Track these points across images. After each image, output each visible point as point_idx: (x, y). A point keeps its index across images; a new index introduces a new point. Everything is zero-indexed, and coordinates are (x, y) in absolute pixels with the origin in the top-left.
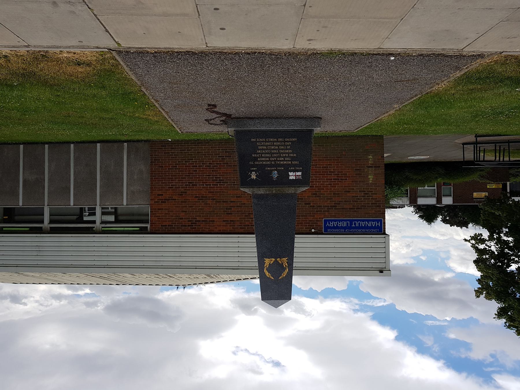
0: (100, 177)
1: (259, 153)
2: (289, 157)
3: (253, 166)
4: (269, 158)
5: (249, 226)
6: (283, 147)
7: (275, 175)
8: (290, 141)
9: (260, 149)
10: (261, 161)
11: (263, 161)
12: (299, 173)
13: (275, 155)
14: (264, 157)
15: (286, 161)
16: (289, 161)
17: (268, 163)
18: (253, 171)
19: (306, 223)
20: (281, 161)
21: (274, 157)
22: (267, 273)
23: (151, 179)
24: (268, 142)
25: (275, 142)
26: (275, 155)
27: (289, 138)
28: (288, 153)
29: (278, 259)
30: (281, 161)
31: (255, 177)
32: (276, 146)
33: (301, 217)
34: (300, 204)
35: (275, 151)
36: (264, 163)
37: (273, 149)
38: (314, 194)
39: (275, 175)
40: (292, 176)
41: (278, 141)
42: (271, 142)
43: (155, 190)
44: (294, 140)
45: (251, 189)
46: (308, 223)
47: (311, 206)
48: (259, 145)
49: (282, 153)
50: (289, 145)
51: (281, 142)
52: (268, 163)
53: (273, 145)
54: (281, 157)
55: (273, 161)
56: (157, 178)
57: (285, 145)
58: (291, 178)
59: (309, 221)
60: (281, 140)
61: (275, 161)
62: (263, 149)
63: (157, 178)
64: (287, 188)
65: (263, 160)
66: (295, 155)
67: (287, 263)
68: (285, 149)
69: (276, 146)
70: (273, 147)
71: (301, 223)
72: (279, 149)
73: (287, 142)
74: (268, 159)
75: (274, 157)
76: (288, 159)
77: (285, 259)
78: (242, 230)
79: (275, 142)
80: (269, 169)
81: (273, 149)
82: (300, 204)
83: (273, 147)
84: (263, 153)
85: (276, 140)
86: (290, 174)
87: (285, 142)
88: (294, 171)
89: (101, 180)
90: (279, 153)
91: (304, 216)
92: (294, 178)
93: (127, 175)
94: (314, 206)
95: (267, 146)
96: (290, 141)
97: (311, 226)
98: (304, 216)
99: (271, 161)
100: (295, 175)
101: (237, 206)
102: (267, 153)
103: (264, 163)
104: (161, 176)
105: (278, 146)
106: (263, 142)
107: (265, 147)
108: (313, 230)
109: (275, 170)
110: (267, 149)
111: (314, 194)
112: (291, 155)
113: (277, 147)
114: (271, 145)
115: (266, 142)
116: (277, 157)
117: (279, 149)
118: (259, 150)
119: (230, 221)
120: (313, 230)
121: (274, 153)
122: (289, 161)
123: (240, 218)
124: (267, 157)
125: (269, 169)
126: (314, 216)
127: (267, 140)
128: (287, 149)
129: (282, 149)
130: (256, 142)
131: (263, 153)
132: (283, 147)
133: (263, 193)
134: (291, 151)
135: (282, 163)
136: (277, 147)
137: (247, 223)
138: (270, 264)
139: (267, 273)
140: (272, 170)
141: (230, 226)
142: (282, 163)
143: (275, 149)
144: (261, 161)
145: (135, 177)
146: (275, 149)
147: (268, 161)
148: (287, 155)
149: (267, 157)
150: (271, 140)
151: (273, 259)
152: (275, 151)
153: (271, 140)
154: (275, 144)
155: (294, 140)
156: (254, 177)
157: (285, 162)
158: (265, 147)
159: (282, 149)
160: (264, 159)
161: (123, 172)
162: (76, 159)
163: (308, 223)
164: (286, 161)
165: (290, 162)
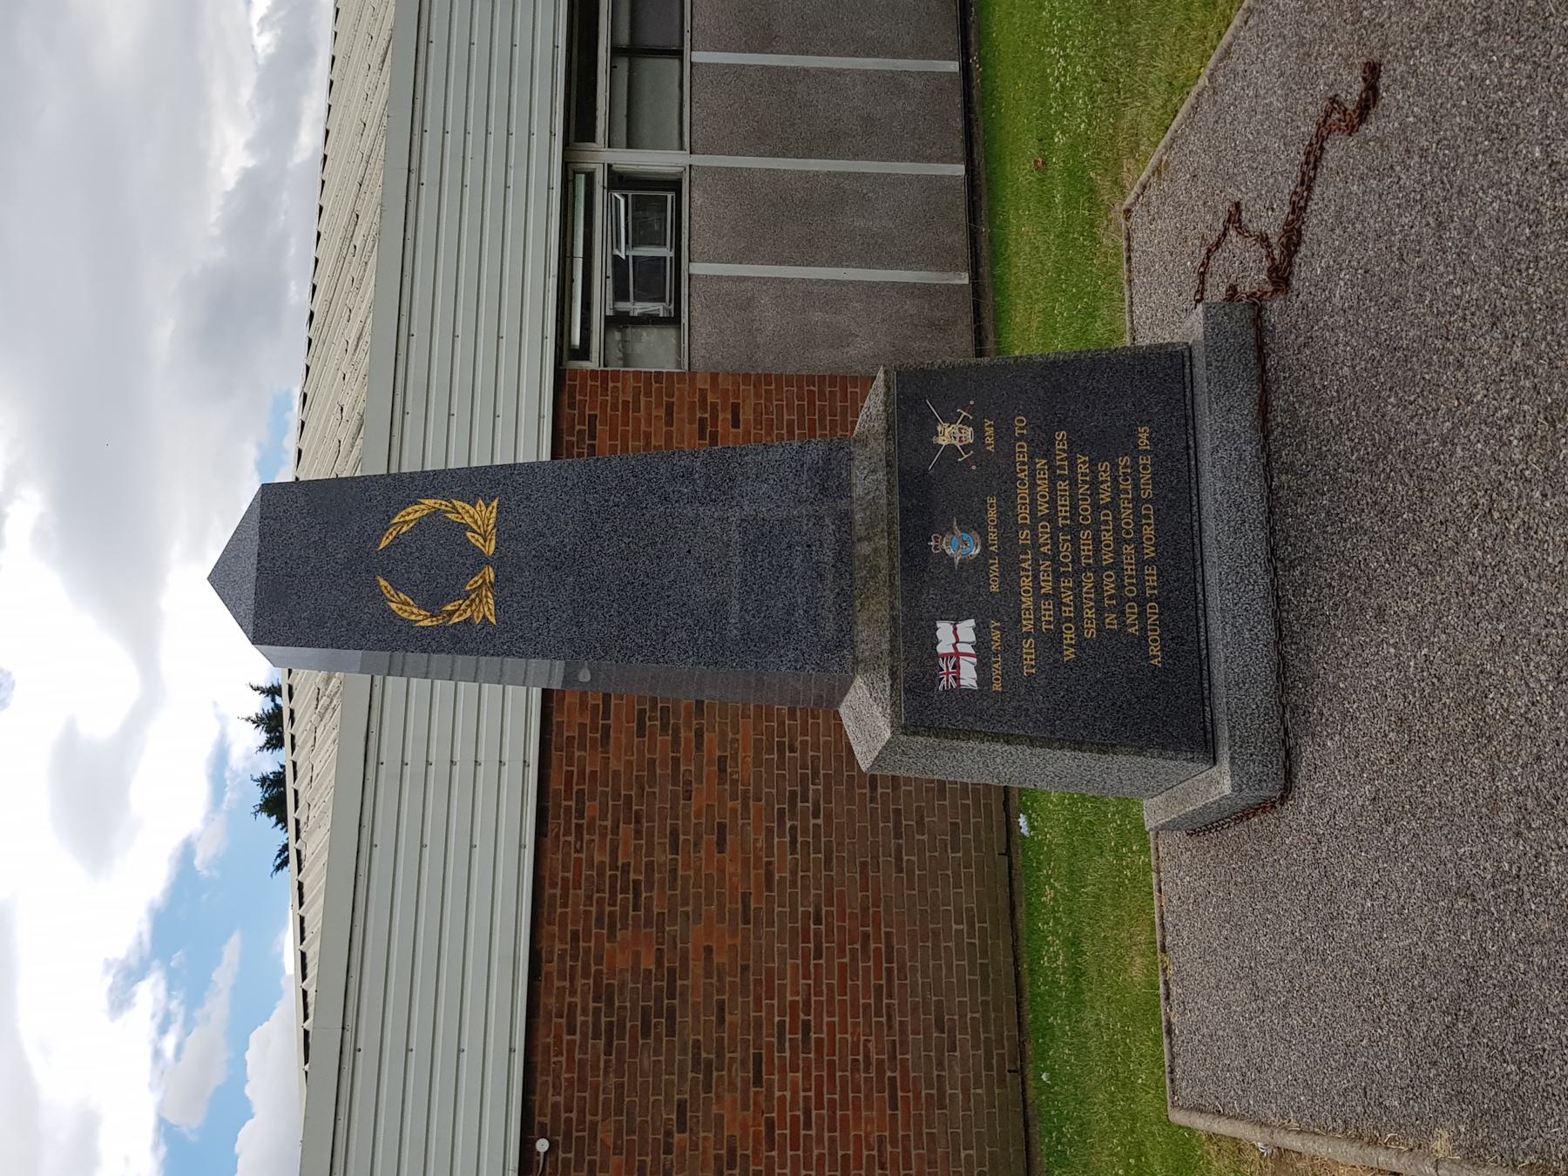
0: (817, 174)
1: (1073, 466)
2: (1059, 621)
3: (1004, 433)
4: (1052, 518)
5: (581, 815)
6: (1110, 589)
7: (960, 546)
8: (1143, 629)
9: (1094, 473)
10: (1032, 476)
11: (1033, 485)
12: (969, 676)
13: (1065, 548)
14: (1053, 489)
15: (1037, 609)
16: (1038, 620)
17: (1024, 513)
18: (979, 433)
19: (582, 1112)
20: (1036, 577)
21: (1055, 544)
22: (413, 513)
23: (810, 380)
24: (1136, 513)
25: (1139, 550)
26: (1065, 548)
27: (1163, 624)
28: (1078, 618)
29: (490, 574)
30: (1036, 577)
31: (943, 441)
32: (1118, 553)
33: (613, 1079)
34: (682, 1075)
35: (1086, 550)
36: (1023, 491)
37: (1097, 540)
38: (732, 1151)
39: (960, 546)
40: (955, 637)
41: (1141, 563)
42: (1138, 529)
43: (758, 396)
44: (1154, 649)
45: (879, 426)
46: (581, 1121)
47: (668, 1134)
48: (1115, 466)
49: (1079, 584)
50: (1123, 625)
51: (1141, 583)
52: (1024, 513)
53: (1119, 541)
54: (1056, 580)
55: (1035, 536)
56: (811, 403)
57: (1121, 600)
58: (944, 630)
59: (594, 1125)
60: (1152, 581)
61: (1035, 546)
62: (1095, 485)
63: (811, 403)
64: (884, 614)
65: (1034, 486)
66: (1070, 654)
67: (468, 622)
68: (1099, 601)
69: (1118, 553)
70: (1107, 537)
71: (582, 1081)
72: (1098, 570)
73: (1142, 614)
74: (1043, 509)
75: (1055, 544)
76: (1047, 615)
77: (487, 609)
78: (557, 784)
79: (1139, 550)
80: (992, 514)
81: (1097, 540)
82: (682, 1075)
83: (1107, 537)
84: (1073, 484)
85: (1149, 552)
86: (967, 629)
87: (1141, 600)
88: (981, 647)
89: (804, 176)
90: (1077, 572)
91: (619, 1099)
92: (941, 649)
93: (826, 282)
94: (668, 1151)
95: (1114, 505)
96: (1143, 629)
97: (568, 1135)
98: (619, 1099)
99: (1033, 528)
100: (958, 654)
101: (676, 761)
102: (1074, 507)
103: (1023, 491)
104: (822, 419)
105: (1116, 566)
106: (1136, 487)
107: (1105, 498)
108: (542, 1145)
109: (985, 546)
110: (1096, 507)
111: (732, 1151)
112: (1069, 636)
113: (1108, 559)
114: (1117, 529)
115: (1137, 500)
116: (1054, 558)
117: (1098, 570)
118: (1093, 464)
119: (606, 728)
120: (542, 1145)
121: (1075, 541)
122: (1038, 620)
123: (616, 773)
124: (1052, 503)
125: (992, 514)
126: (618, 1150)
127: (1148, 510)
128: (1100, 611)
129: (1098, 587)
130: (1135, 453)
131: (1073, 484)
132: (1110, 589)
133: (858, 491)
134: (1090, 632)
135: (1026, 583)
136: (1108, 559)
137: (592, 808)
138: (467, 527)
139: (413, 513)
140: (984, 536)
141: (583, 726)
142: (1026, 583)
143: (1097, 550)
144: (1032, 476)
145: (817, 316)
146: (1097, 550)
147: (1033, 514)
148: (1068, 612)
149: (1052, 503)
150: (1148, 531)
151: (490, 548)
152: (1086, 550)
153: (1148, 531)
154: (1128, 549)
155: (1154, 649)
156: (948, 435)
157: (1027, 601)
158: (1105, 498)
159: (1098, 587)
160: (1043, 487)
161: (839, 264)
162: (894, 82)
163: (581, 1121)
164: (1037, 609)
165: (1027, 626)
